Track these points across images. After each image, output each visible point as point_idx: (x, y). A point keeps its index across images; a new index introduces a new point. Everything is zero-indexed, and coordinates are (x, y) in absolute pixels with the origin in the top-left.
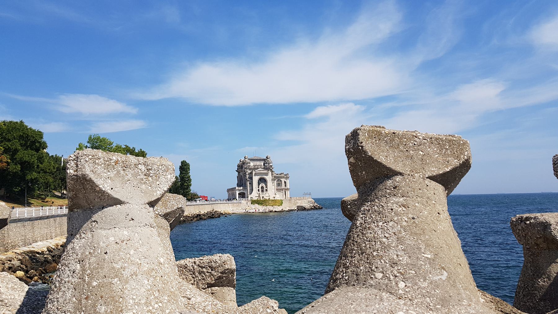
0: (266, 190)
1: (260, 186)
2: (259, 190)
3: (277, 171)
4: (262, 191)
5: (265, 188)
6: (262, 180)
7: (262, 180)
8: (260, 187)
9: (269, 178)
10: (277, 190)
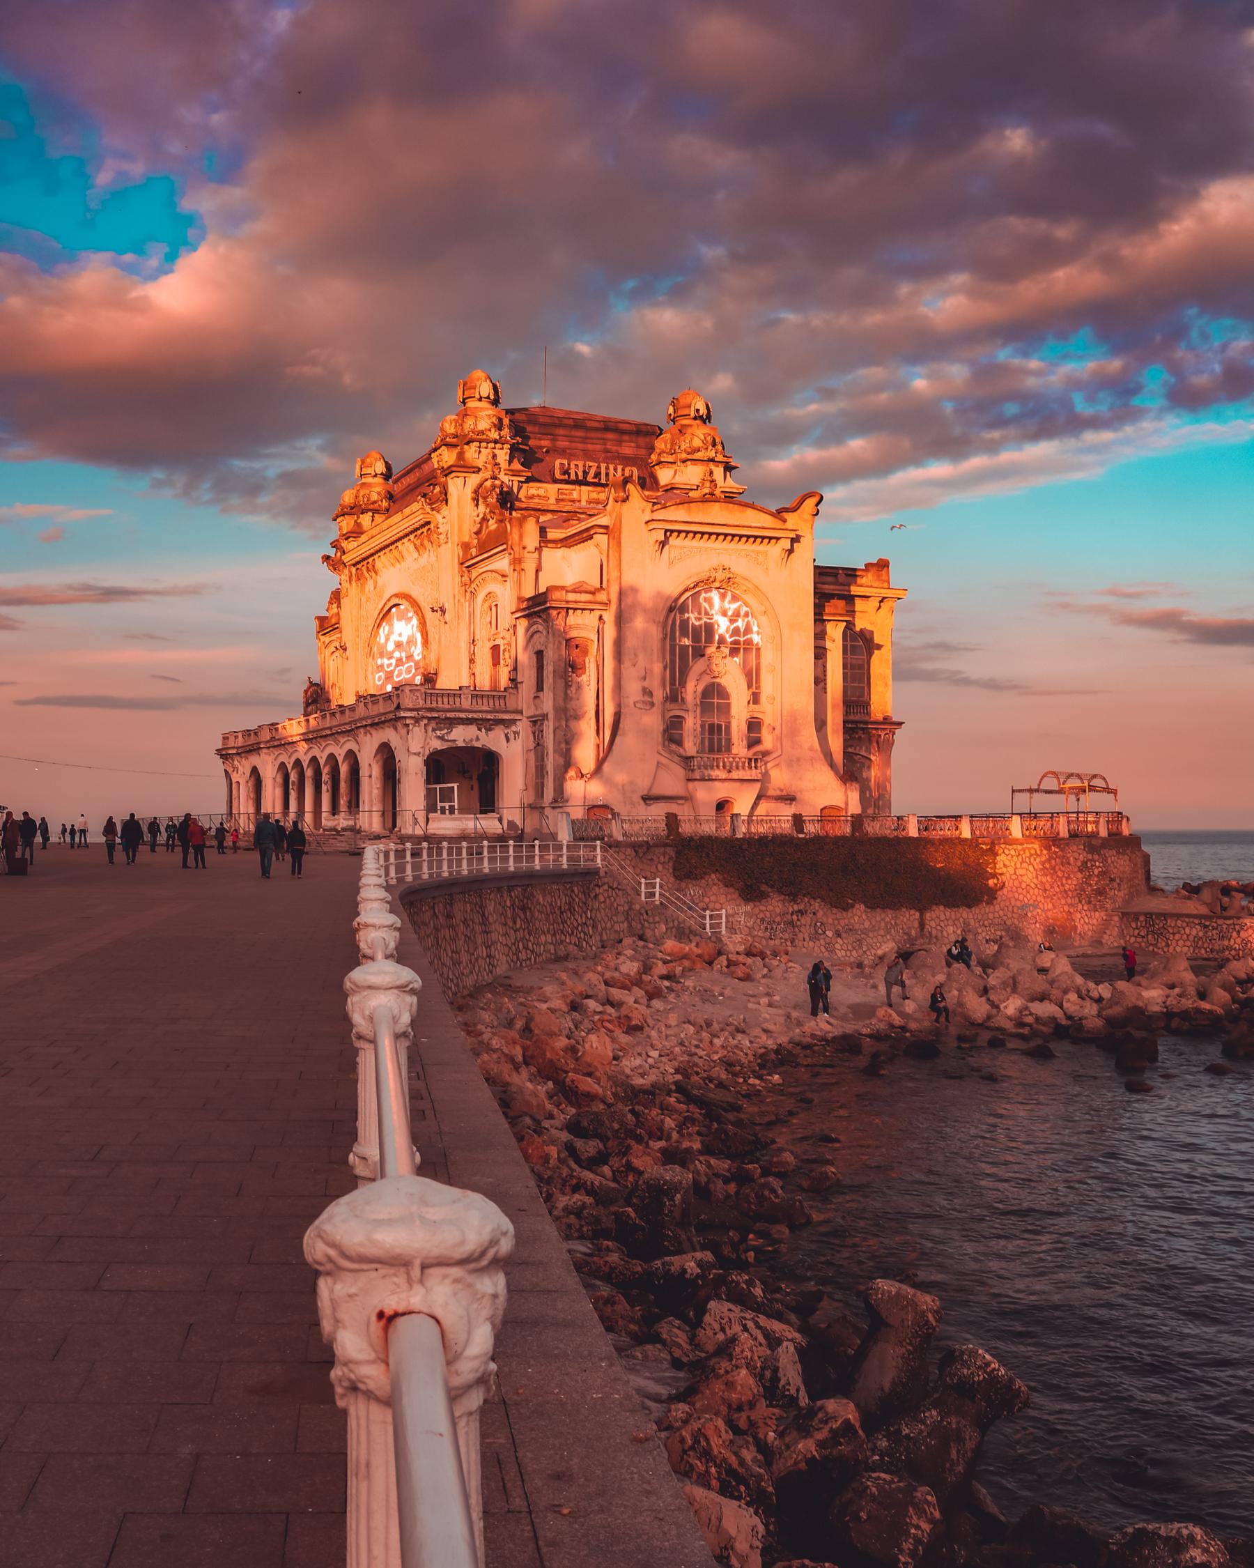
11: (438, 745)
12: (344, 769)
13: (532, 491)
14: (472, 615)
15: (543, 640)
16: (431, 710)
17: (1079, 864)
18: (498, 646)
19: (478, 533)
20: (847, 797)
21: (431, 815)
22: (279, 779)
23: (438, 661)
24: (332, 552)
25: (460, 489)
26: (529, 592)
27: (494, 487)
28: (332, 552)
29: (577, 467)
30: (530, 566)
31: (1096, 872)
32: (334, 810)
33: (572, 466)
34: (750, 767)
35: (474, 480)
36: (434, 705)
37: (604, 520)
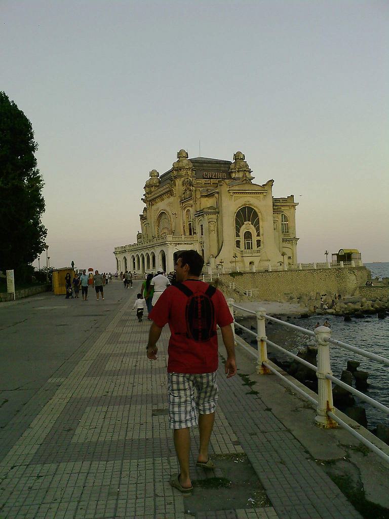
0: (259, 242)
1: (243, 230)
2: (238, 243)
3: (278, 192)
4: (249, 246)
5: (255, 238)
6: (247, 214)
7: (247, 214)
8: (242, 233)
9: (263, 206)
10: (284, 240)
12: (151, 257)
22: (132, 260)
23: (175, 227)
24: (144, 197)
25: (179, 182)
27: (188, 181)
28: (144, 197)
29: (209, 175)
30: (198, 203)
32: (148, 267)
35: (183, 179)
37: (217, 191)
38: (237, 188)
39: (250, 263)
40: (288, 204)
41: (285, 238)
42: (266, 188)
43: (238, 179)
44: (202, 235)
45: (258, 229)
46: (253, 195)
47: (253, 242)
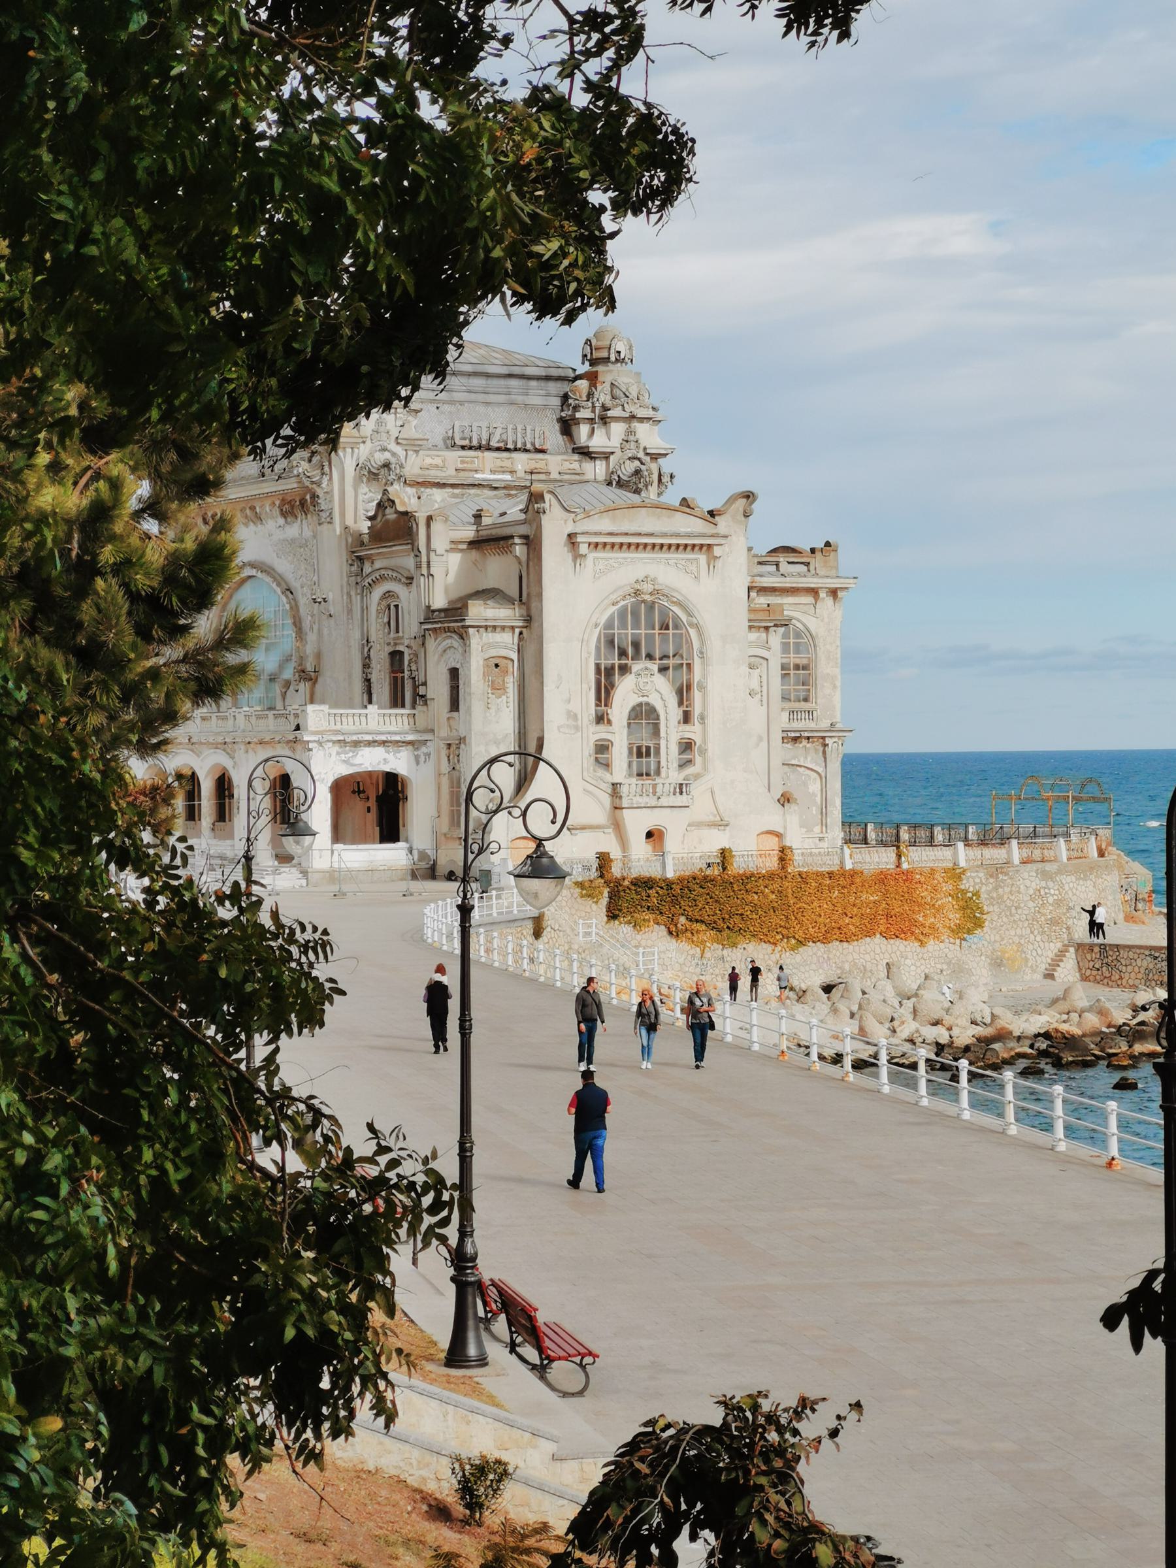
1: (626, 694)
2: (602, 748)
5: (672, 732)
9: (713, 595)
11: (345, 771)
13: (428, 461)
14: (365, 609)
15: (458, 656)
16: (337, 732)
17: (1031, 892)
18: (401, 653)
19: (371, 518)
20: (785, 821)
21: (336, 846)
23: (318, 656)
26: (439, 601)
31: (1051, 900)
33: (474, 429)
34: (681, 793)
36: (338, 727)
38: (604, 524)
39: (649, 835)
40: (812, 582)
41: (796, 725)
42: (723, 523)
43: (606, 456)
44: (455, 705)
45: (683, 693)
46: (673, 556)
47: (663, 743)
